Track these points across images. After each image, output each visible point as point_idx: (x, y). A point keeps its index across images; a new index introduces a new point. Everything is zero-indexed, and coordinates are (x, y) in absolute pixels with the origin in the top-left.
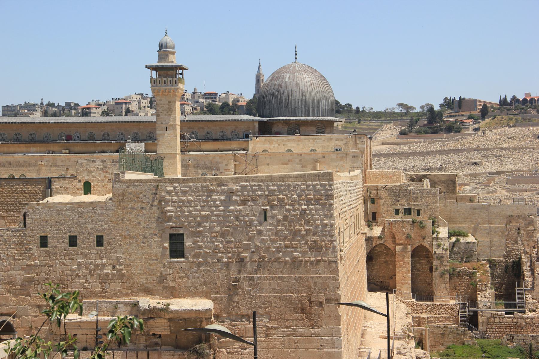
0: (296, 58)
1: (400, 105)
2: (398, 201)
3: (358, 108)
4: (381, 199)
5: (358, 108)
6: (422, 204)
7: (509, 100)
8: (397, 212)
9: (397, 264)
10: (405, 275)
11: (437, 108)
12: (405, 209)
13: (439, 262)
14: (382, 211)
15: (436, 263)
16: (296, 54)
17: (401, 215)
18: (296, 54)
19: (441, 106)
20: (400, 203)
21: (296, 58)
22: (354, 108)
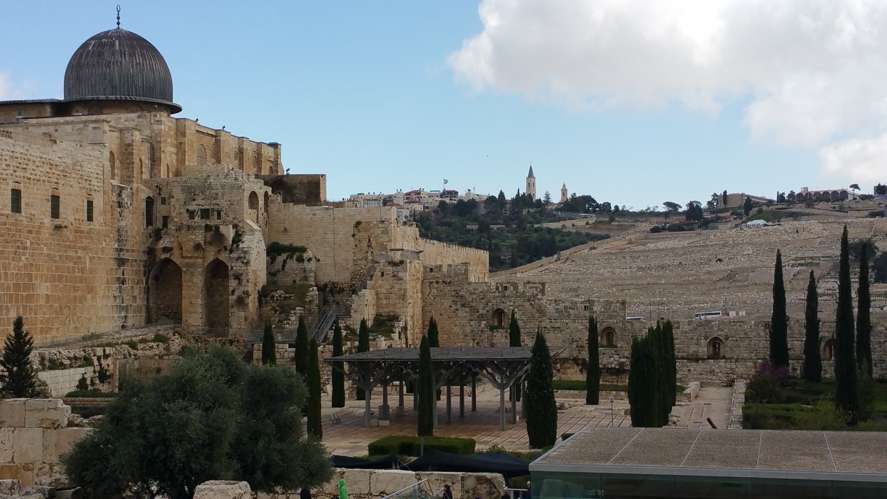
0: (118, 23)
1: (668, 204)
2: (194, 200)
3: (616, 207)
4: (173, 197)
5: (616, 207)
6: (223, 203)
7: (786, 196)
8: (192, 214)
9: (184, 284)
10: (194, 301)
11: (704, 205)
12: (202, 210)
13: (237, 281)
14: (174, 214)
15: (233, 283)
16: (118, 18)
17: (197, 219)
18: (118, 18)
19: (709, 203)
20: (196, 202)
21: (118, 23)
22: (613, 208)
